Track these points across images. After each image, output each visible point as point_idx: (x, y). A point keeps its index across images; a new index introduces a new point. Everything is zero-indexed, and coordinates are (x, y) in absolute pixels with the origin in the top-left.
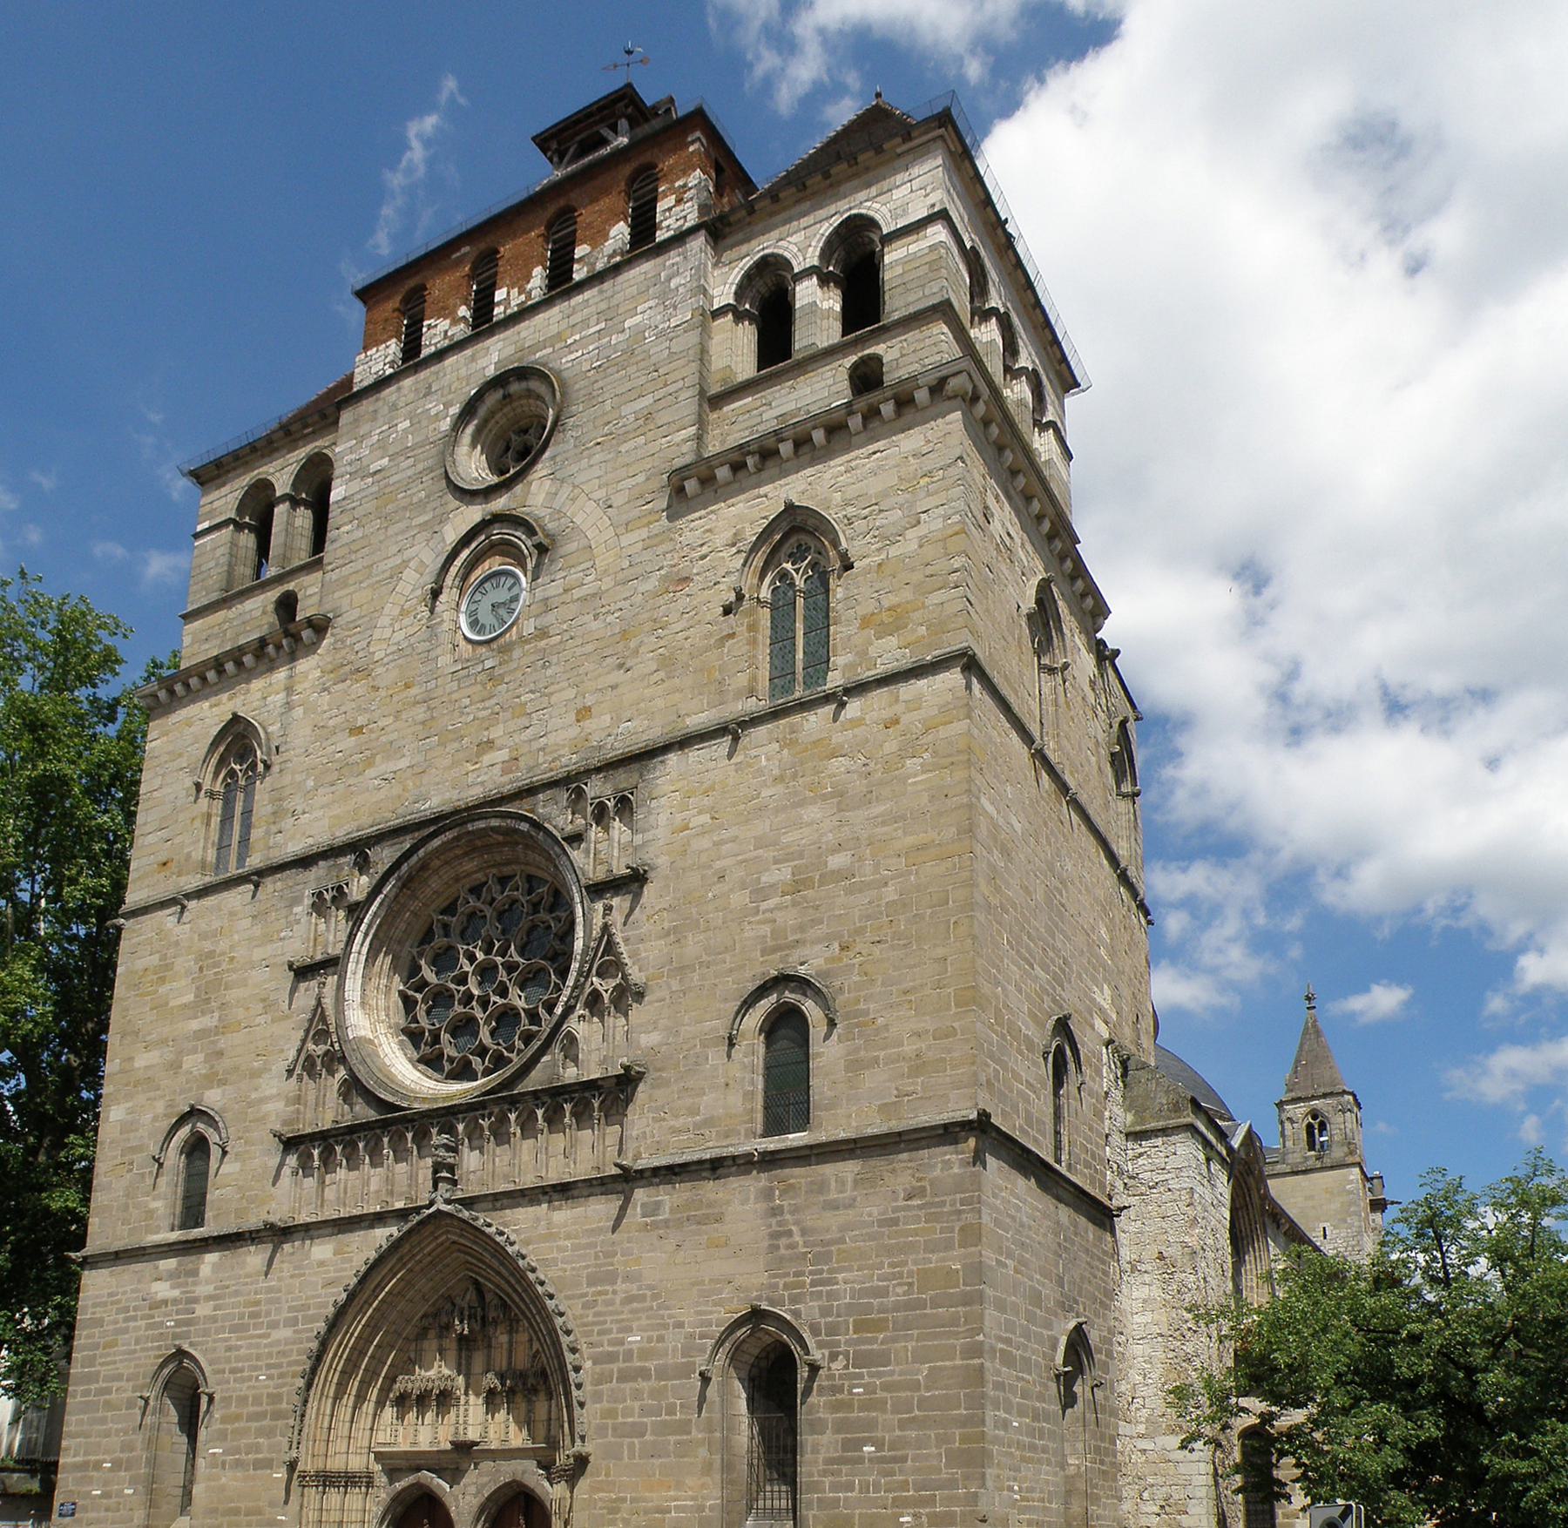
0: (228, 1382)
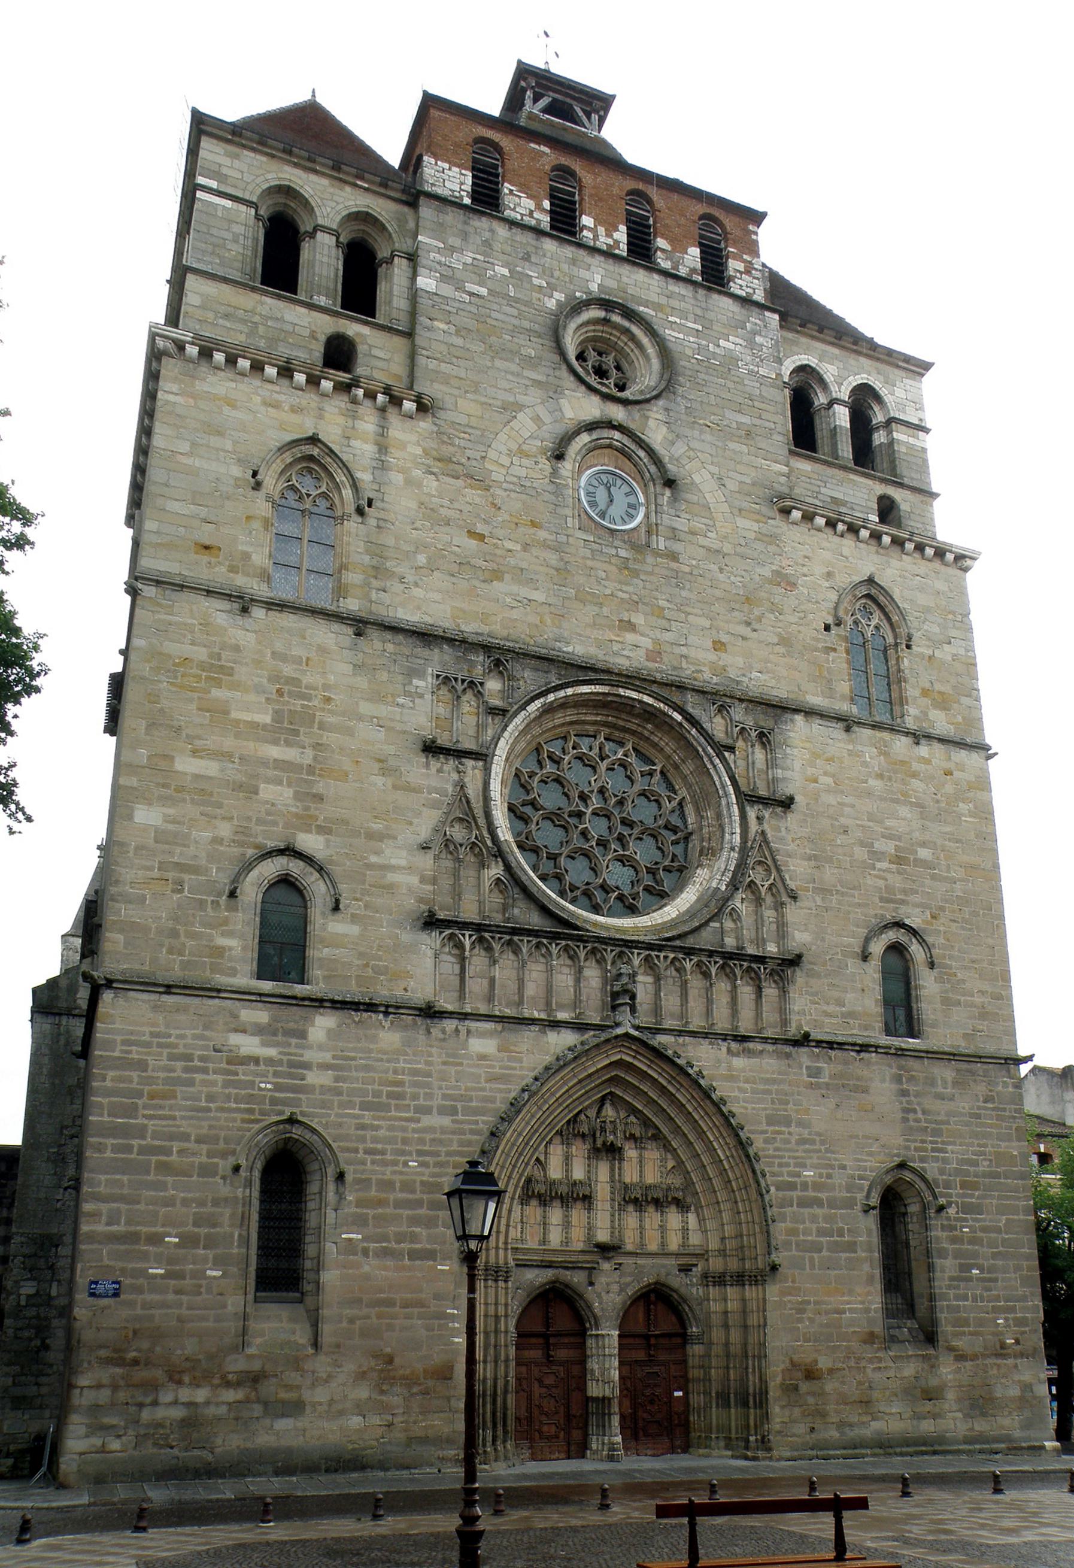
0: (364, 1163)
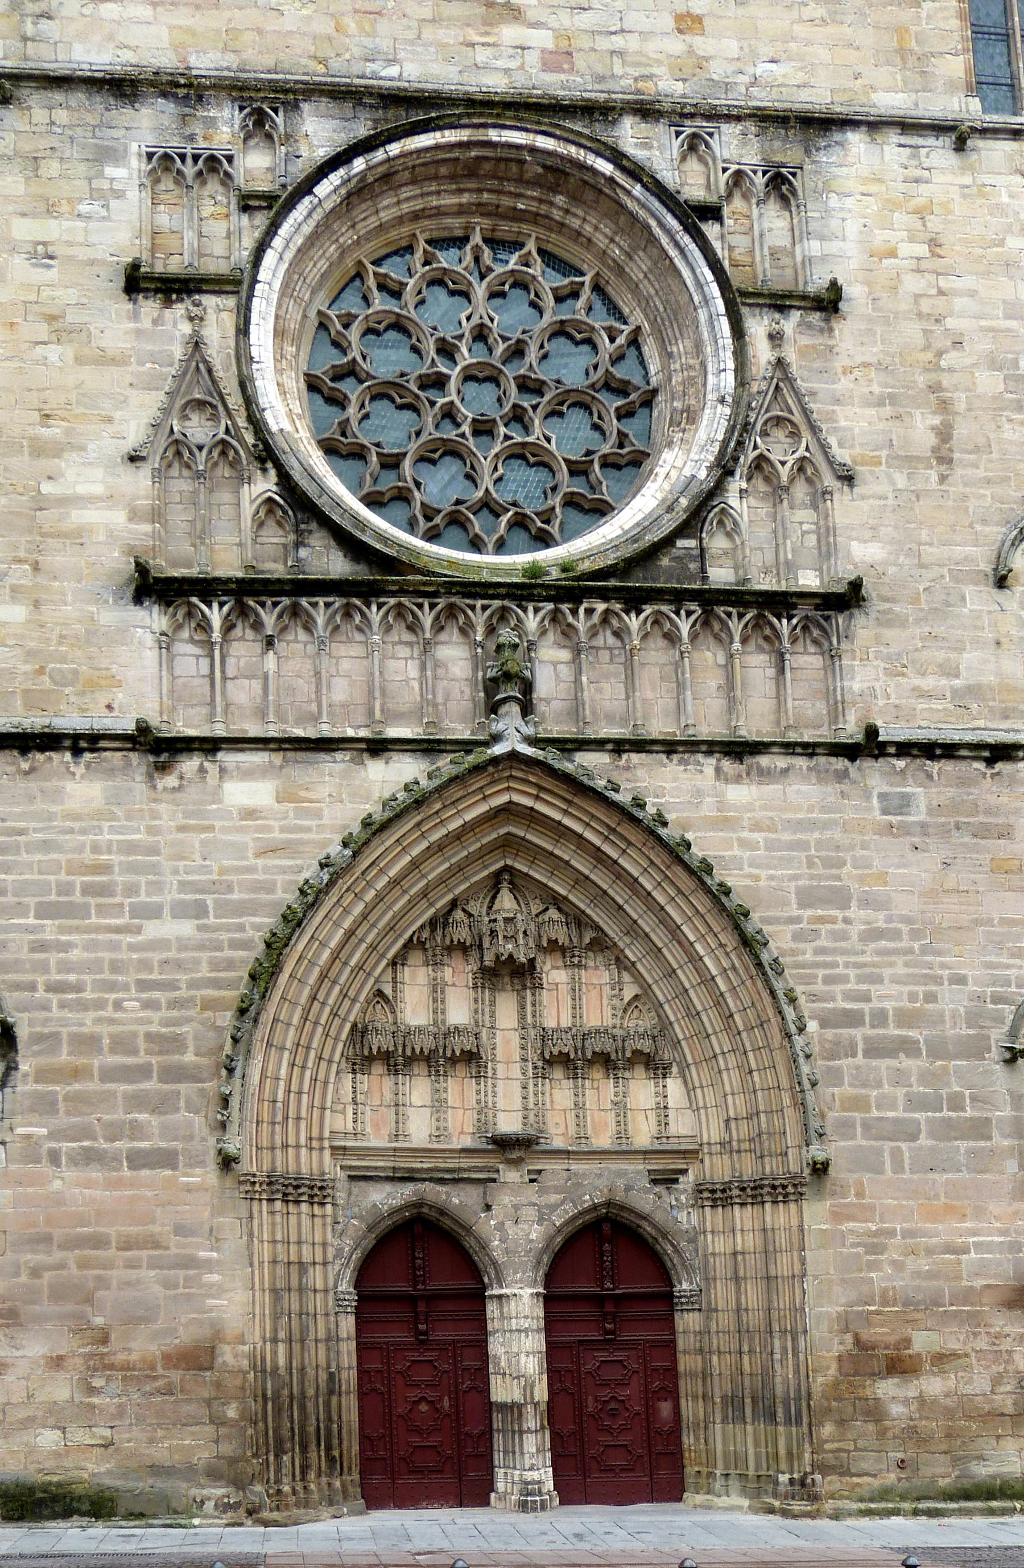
0: (46, 1008)
